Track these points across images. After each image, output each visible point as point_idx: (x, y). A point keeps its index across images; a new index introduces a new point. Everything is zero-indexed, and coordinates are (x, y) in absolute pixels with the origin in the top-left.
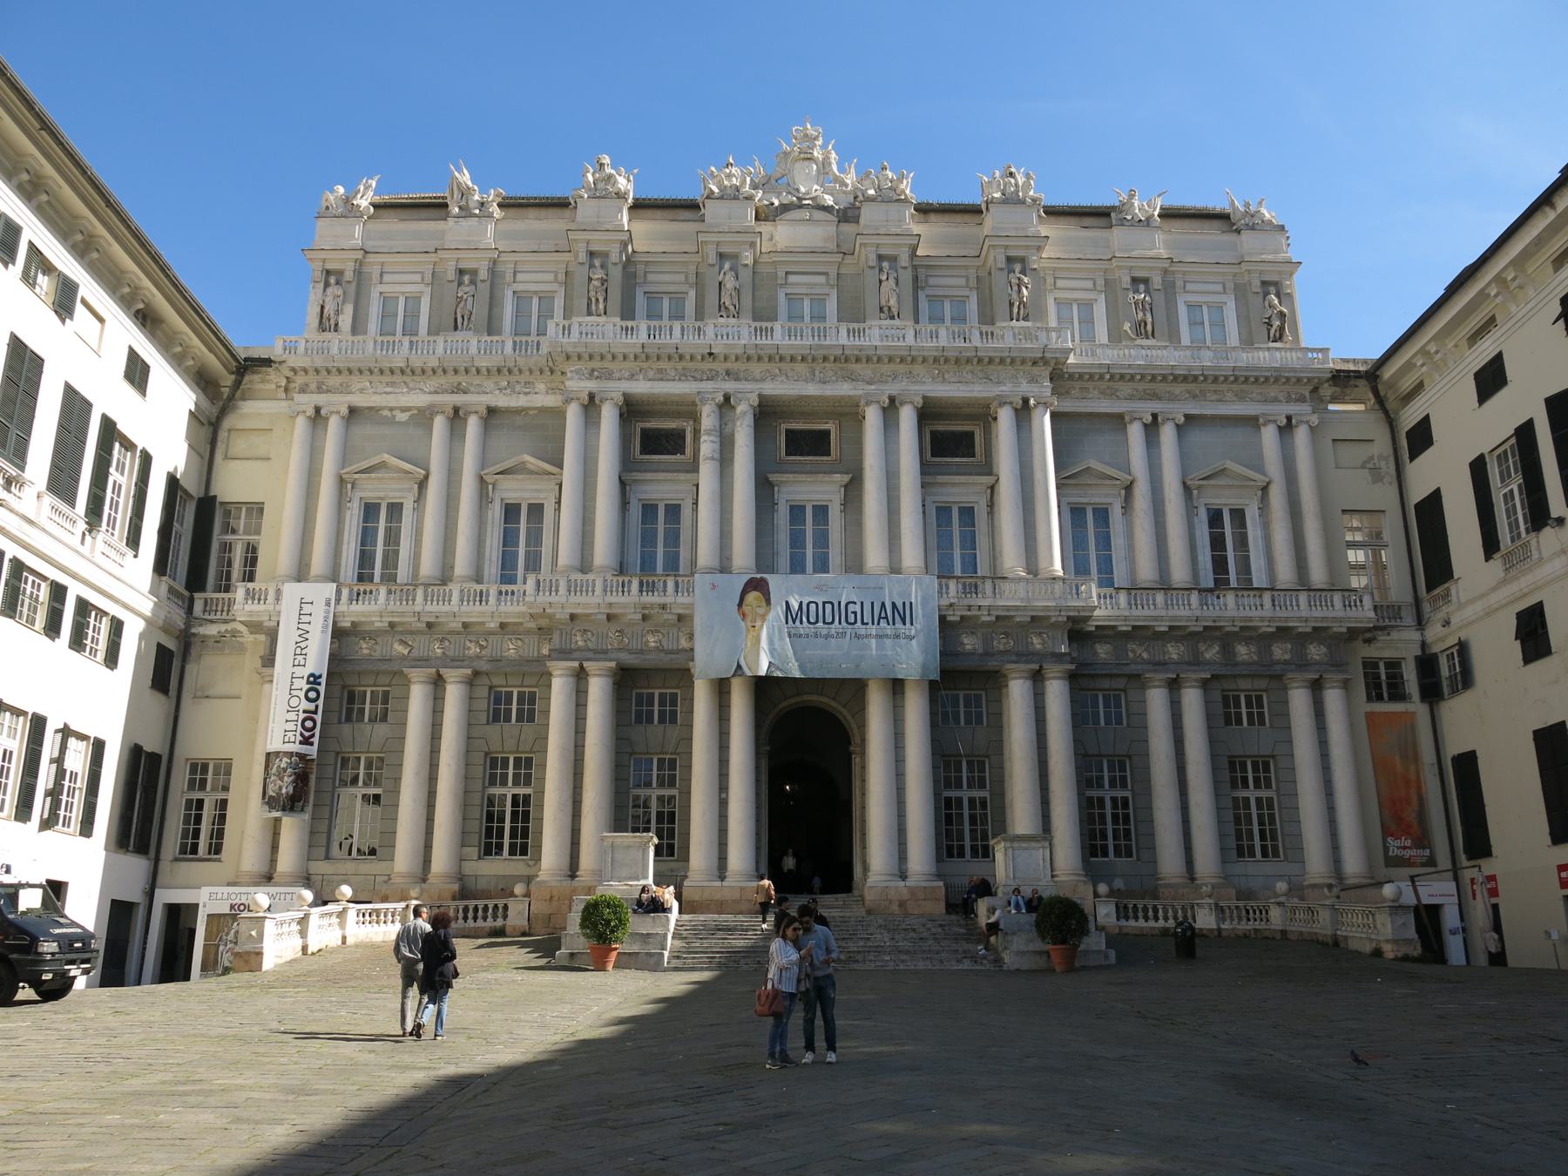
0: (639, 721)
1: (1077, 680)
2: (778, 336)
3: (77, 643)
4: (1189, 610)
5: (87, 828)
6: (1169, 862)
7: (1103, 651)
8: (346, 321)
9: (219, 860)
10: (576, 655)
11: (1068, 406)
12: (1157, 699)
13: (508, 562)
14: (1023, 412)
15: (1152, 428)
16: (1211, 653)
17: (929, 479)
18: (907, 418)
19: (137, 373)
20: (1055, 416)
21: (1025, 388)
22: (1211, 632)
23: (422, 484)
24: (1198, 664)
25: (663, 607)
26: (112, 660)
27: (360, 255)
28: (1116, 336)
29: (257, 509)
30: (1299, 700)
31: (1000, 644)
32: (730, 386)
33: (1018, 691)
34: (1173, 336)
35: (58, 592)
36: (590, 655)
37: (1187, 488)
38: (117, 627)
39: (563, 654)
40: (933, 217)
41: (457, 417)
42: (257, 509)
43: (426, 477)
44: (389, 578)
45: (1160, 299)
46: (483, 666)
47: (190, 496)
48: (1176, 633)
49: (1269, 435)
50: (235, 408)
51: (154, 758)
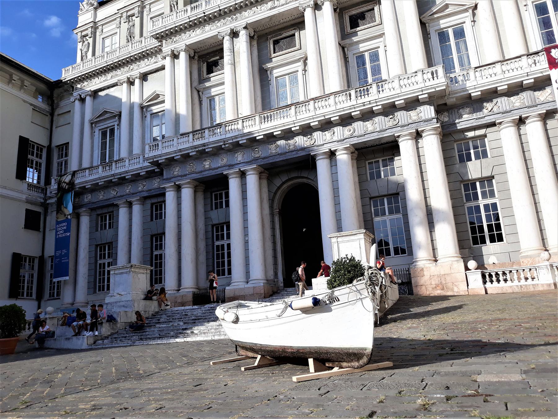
0: (216, 208)
9: (59, 299)
10: (173, 180)
17: (347, 41)
23: (120, 115)
24: (536, 106)
25: (204, 145)
27: (92, 25)
36: (180, 178)
39: (168, 180)
43: (121, 113)
46: (145, 194)
47: (44, 147)
50: (58, 106)
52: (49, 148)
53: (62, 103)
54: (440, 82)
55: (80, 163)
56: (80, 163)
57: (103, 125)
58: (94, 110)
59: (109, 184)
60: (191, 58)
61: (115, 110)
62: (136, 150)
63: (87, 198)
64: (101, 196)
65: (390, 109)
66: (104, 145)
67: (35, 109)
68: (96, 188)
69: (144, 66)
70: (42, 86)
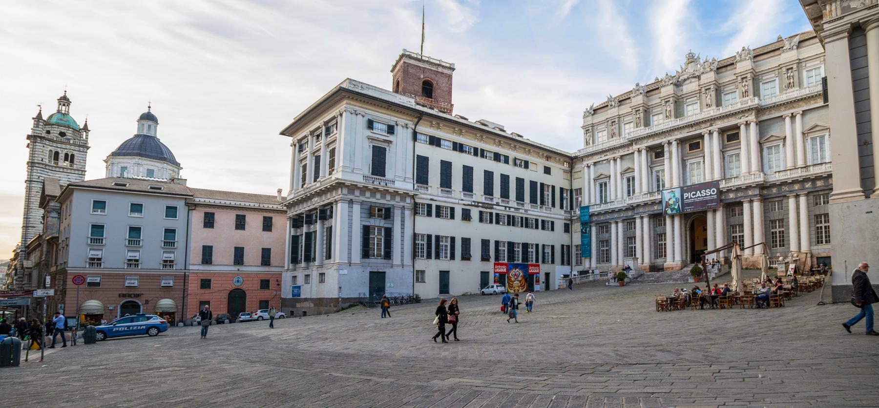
3: (543, 228)
4: (798, 174)
5: (553, 262)
8: (591, 142)
11: (765, 117)
18: (715, 135)
19: (547, 170)
20: (759, 124)
21: (747, 119)
26: (553, 229)
29: (580, 189)
31: (739, 195)
32: (669, 138)
33: (746, 206)
34: (800, 85)
35: (537, 220)
37: (803, 134)
38: (553, 223)
39: (637, 214)
40: (729, 68)
41: (615, 160)
42: (580, 189)
44: (605, 201)
45: (796, 74)
51: (568, 246)
52: (571, 191)
53: (577, 166)
54: (760, 179)
55: (590, 201)
56: (590, 201)
57: (601, 181)
58: (595, 172)
59: (606, 213)
60: (647, 151)
61: (607, 174)
62: (619, 196)
63: (595, 219)
64: (602, 218)
66: (601, 191)
67: (565, 171)
68: (599, 214)
69: (622, 152)
70: (567, 160)
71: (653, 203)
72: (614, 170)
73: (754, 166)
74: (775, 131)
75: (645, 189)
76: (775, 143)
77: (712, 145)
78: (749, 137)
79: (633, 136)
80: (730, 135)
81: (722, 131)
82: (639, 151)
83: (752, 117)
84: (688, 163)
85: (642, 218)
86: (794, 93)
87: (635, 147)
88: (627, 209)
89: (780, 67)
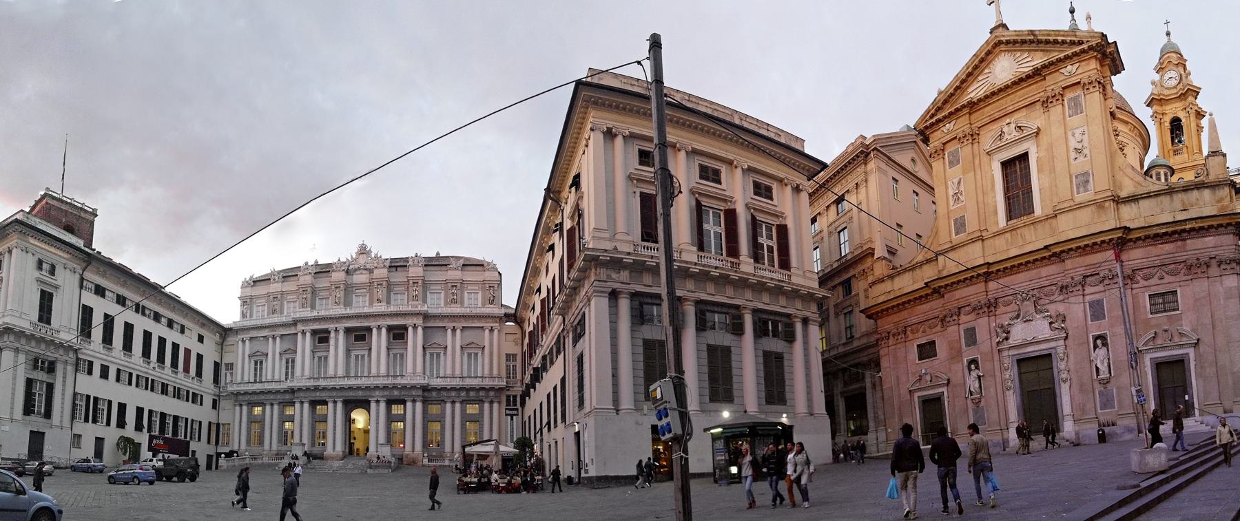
1: (425, 402)
2: (349, 311)
4: (456, 383)
6: (448, 448)
7: (434, 394)
12: (448, 406)
13: (287, 374)
14: (415, 327)
15: (454, 330)
16: (463, 394)
18: (384, 331)
20: (425, 328)
22: (462, 389)
28: (446, 303)
30: (486, 406)
34: (462, 303)
48: (453, 389)
49: (487, 331)
59: (262, 393)
62: (277, 377)
65: (404, 387)
68: (254, 393)
71: (316, 389)
72: (274, 348)
73: (419, 369)
74: (438, 338)
75: (307, 373)
76: (437, 351)
77: (379, 340)
78: (415, 339)
79: (298, 315)
80: (398, 334)
81: (390, 329)
82: (304, 333)
83: (419, 321)
84: (353, 354)
85: (302, 403)
86: (456, 310)
87: (300, 327)
88: (285, 392)
89: (446, 282)
